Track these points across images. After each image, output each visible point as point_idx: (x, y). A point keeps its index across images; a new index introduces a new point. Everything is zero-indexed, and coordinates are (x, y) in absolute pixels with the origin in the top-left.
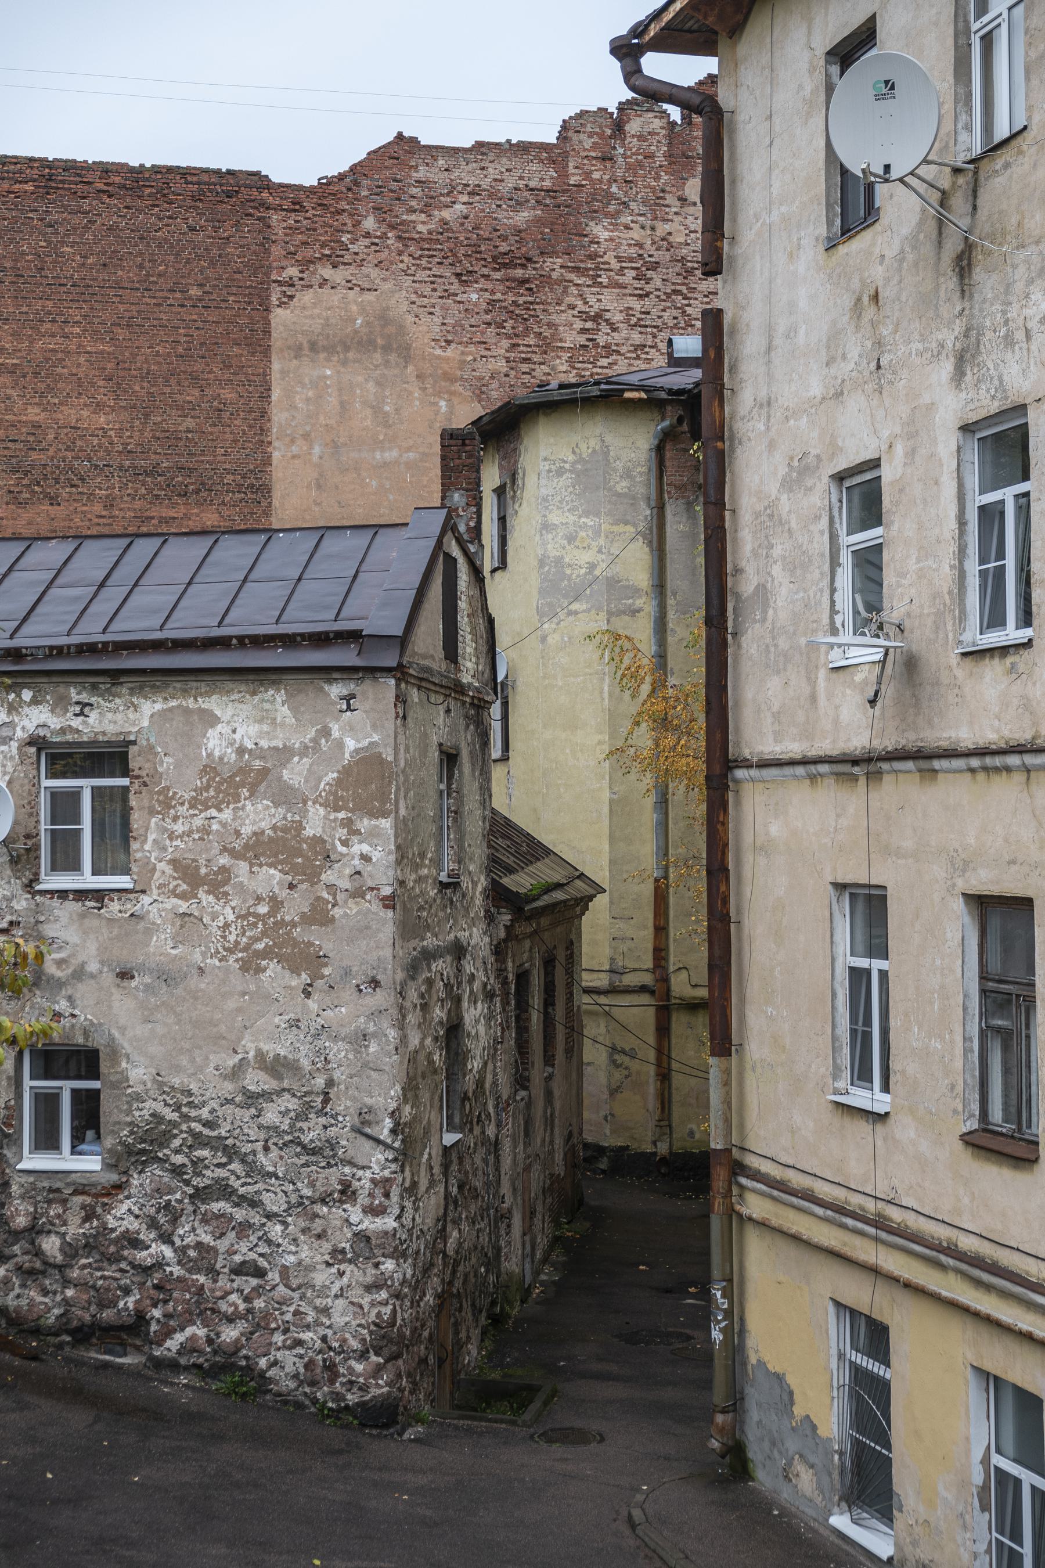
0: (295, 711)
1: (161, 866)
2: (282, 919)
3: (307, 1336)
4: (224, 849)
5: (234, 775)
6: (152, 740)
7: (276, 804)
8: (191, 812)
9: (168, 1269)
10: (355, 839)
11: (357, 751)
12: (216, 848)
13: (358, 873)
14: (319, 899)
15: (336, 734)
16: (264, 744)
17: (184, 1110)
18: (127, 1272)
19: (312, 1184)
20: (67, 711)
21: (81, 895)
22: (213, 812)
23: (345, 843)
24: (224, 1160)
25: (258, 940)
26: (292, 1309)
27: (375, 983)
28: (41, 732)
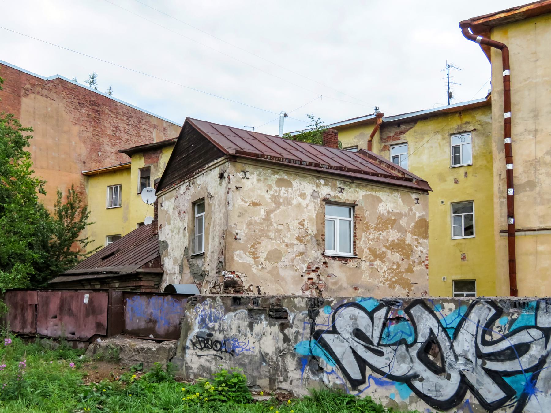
0: (403, 200)
1: (366, 250)
4: (384, 246)
5: (386, 221)
6: (363, 205)
7: (399, 232)
10: (419, 245)
11: (419, 217)
12: (382, 245)
14: (410, 264)
15: (414, 210)
16: (395, 211)
20: (336, 190)
21: (341, 258)
22: (381, 232)
23: (416, 247)
28: (328, 197)
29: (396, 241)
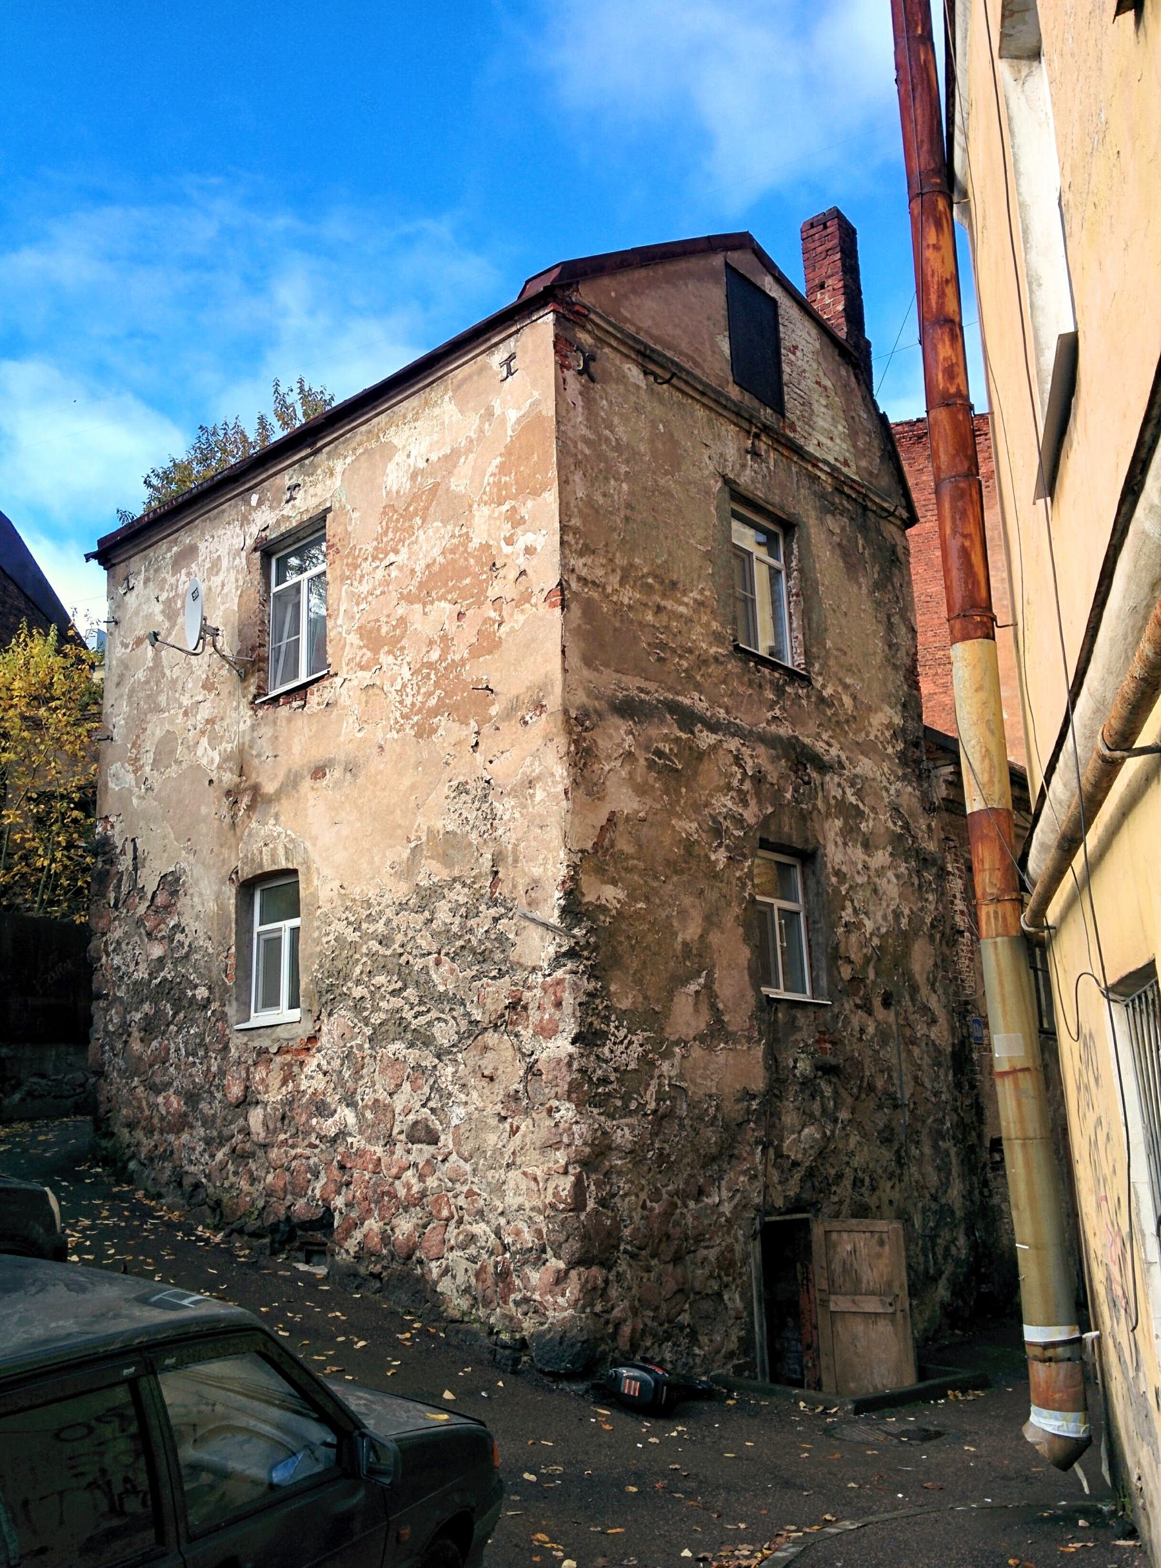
2: (453, 661)
3: (479, 1228)
6: (343, 499)
8: (374, 565)
9: (350, 1140)
11: (518, 421)
13: (523, 573)
14: (486, 620)
15: (498, 411)
16: (434, 457)
17: (364, 926)
18: (316, 1147)
19: (481, 1004)
22: (392, 557)
23: (510, 541)
24: (400, 984)
25: (430, 694)
26: (465, 1188)
27: (540, 707)
29: (441, 559)
